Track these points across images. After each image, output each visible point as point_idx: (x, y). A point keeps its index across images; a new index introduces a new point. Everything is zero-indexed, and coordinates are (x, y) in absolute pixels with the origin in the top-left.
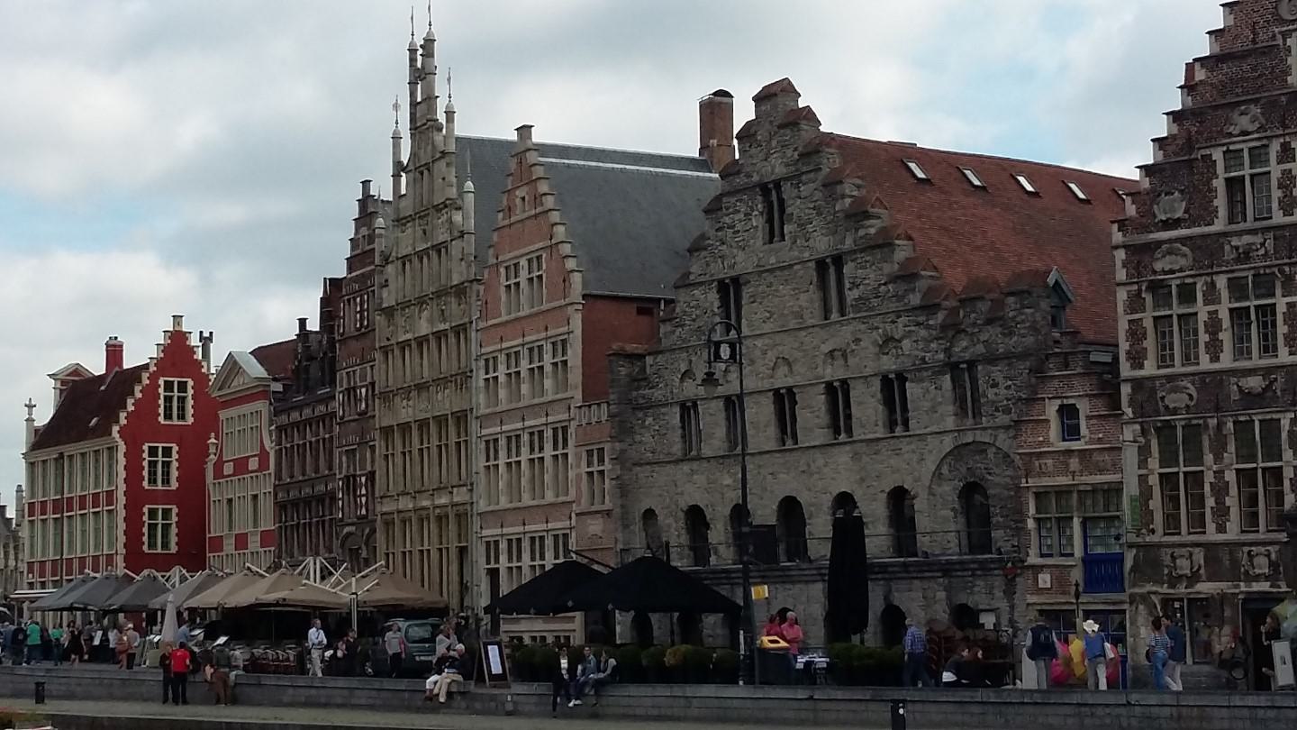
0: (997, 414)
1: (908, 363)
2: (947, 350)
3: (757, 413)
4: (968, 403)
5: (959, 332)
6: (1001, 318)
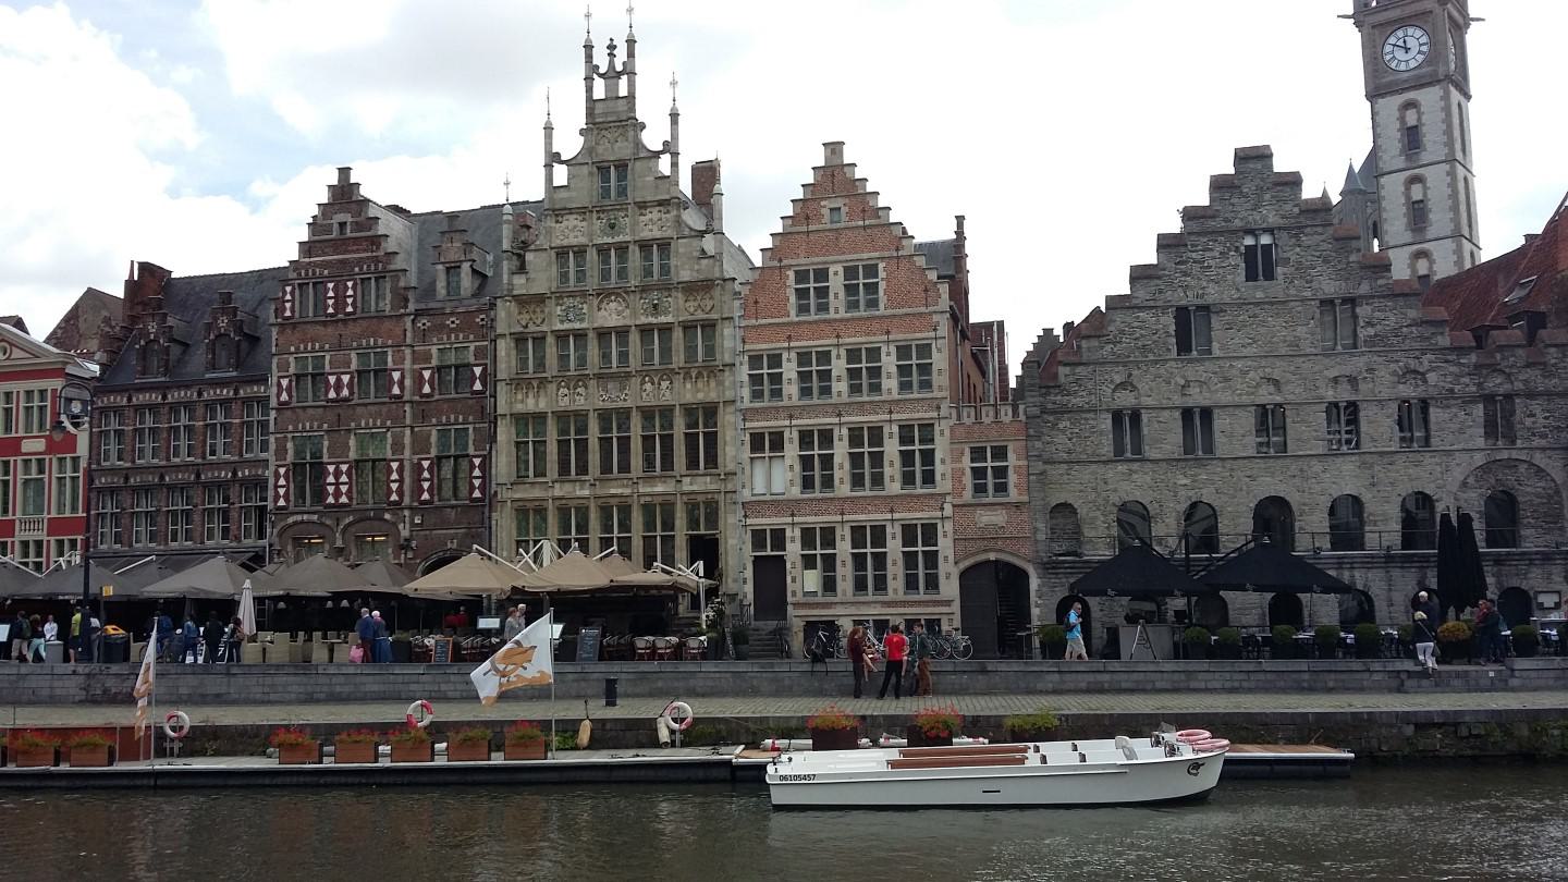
0: (1533, 438)
1: (1433, 392)
2: (1479, 385)
3: (1230, 424)
4: (1499, 425)
5: (1494, 371)
6: (1545, 364)
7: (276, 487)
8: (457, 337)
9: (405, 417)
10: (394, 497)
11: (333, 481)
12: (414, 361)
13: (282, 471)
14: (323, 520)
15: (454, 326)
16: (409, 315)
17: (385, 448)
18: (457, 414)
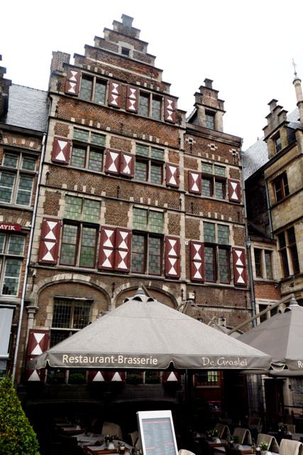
7: (42, 240)
8: (216, 158)
9: (180, 204)
10: (172, 272)
11: (111, 245)
12: (186, 163)
13: (52, 225)
14: (97, 283)
15: (212, 149)
16: (183, 129)
17: (163, 227)
18: (220, 213)
